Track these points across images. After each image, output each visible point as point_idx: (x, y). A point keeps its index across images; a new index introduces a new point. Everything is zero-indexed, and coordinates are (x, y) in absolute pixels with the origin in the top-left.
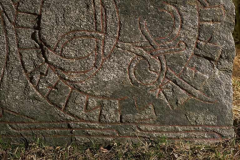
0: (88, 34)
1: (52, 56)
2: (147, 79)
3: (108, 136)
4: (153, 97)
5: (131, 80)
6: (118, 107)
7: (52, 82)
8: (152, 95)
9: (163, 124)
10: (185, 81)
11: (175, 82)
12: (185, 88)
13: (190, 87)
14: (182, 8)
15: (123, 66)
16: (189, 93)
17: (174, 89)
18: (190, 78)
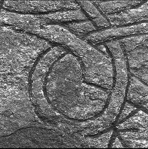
15: (16, 73)
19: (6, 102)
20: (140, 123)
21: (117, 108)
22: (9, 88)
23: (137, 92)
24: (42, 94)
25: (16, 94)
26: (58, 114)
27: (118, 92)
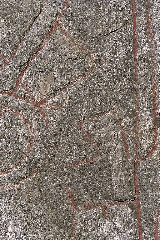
2: (18, 138)
4: (63, 122)
5: (19, 179)
6: (95, 211)
8: (59, 124)
9: (133, 92)
10: (19, 42)
11: (22, 68)
12: (38, 40)
13: (35, 32)
16: (51, 29)
17: (42, 68)
18: (10, 30)
19: (15, 211)
20: (34, 79)
21: (20, 102)
22: (2, 208)
23: (4, 83)
24: (7, 176)
25: (7, 201)
26: (26, 159)
27: (5, 102)
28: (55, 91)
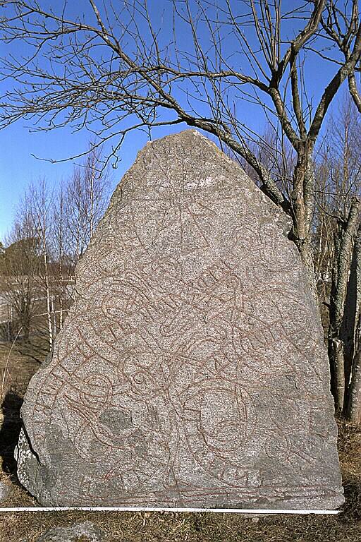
0: (235, 423)
1: (210, 441)
3: (253, 497)
7: (211, 459)
9: (292, 486)
14: (298, 400)
28: (292, 463)
